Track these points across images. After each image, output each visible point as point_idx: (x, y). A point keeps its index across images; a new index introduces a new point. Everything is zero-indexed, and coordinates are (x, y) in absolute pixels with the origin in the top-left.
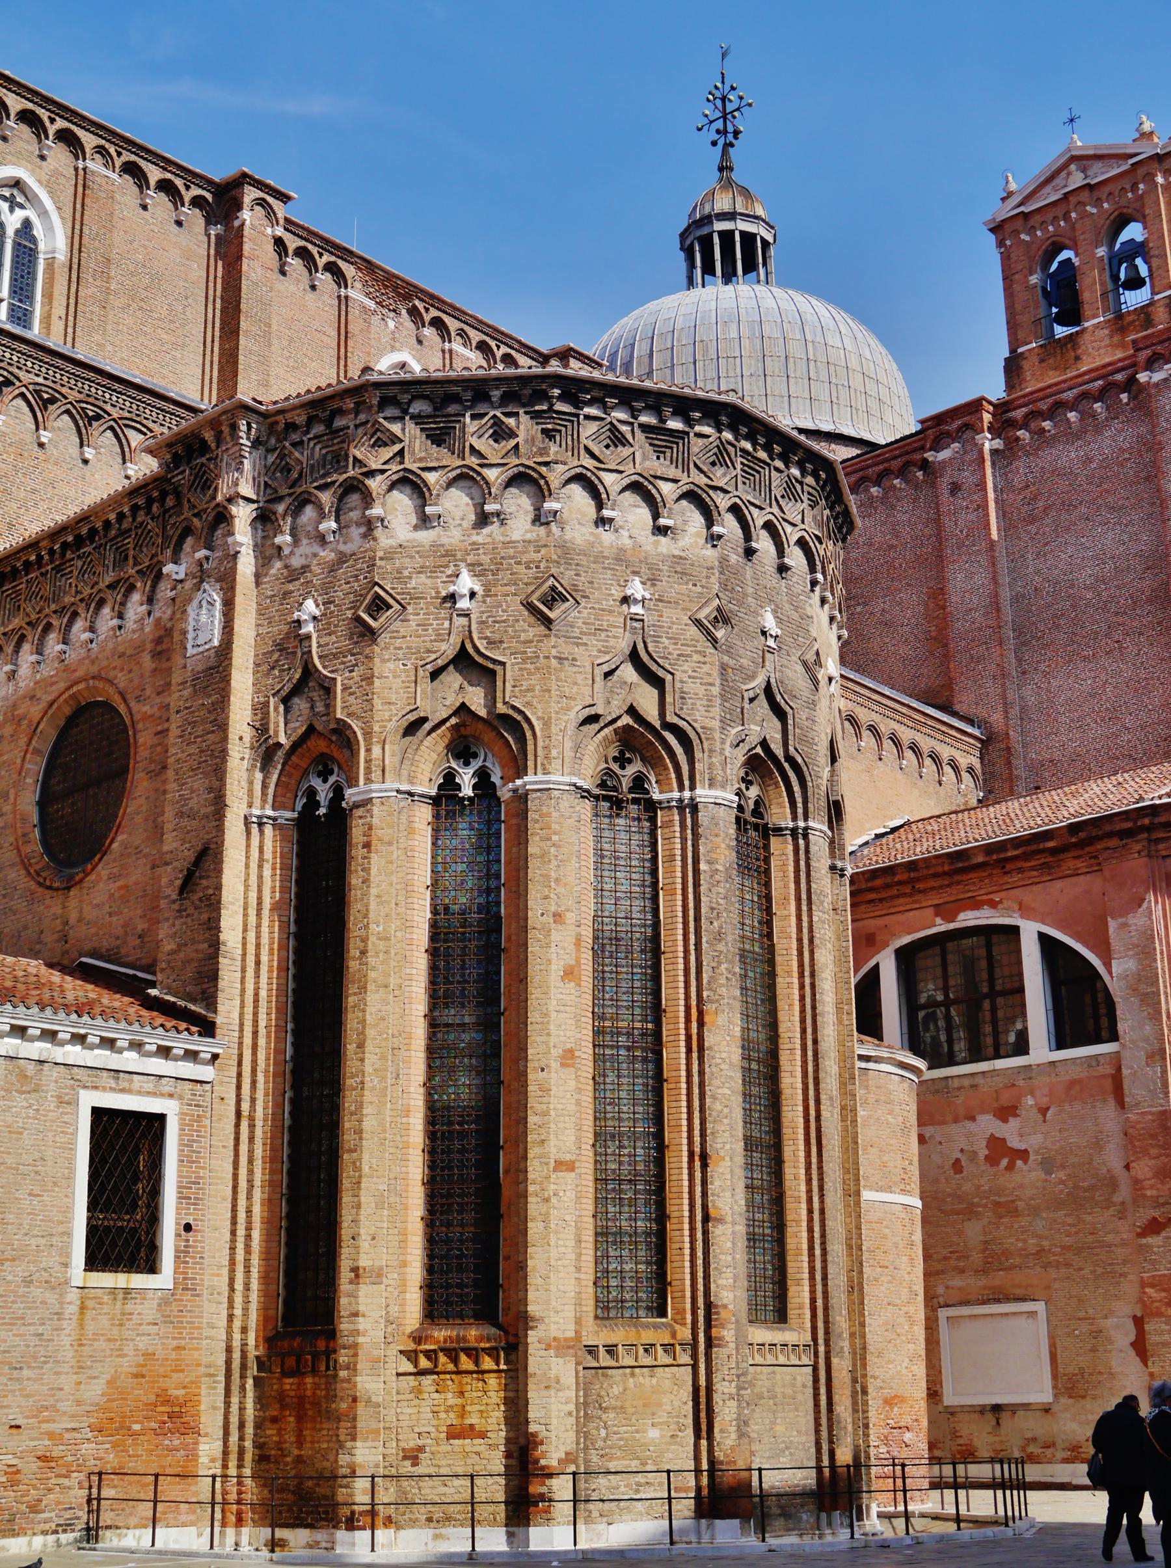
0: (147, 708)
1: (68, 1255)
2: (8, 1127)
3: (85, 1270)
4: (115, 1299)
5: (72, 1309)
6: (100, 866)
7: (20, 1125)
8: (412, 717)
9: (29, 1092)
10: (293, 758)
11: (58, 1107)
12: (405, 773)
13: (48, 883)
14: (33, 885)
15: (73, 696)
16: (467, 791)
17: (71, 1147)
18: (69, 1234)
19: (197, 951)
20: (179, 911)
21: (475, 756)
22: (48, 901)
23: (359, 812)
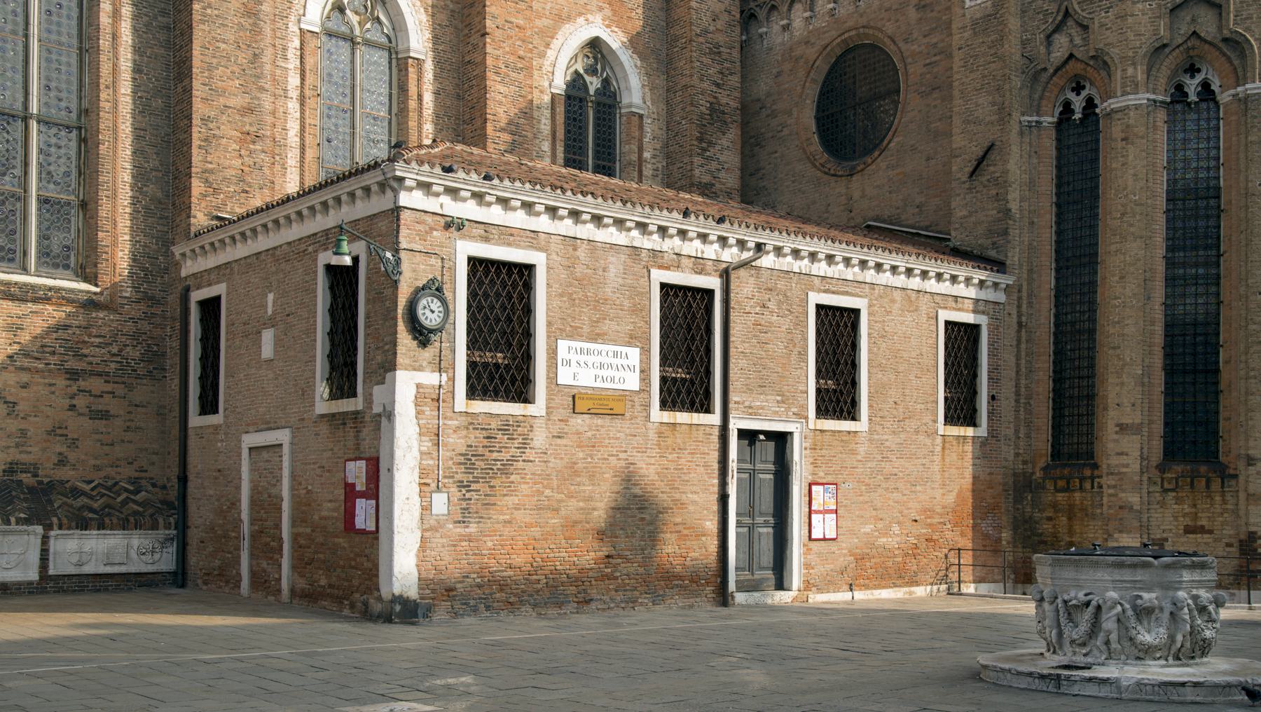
0: (916, 46)
5: (939, 449)
6: (879, 160)
8: (1157, 45)
10: (1054, 78)
12: (1151, 86)
13: (832, 172)
14: (819, 174)
15: (844, 41)
16: (1193, 97)
21: (1199, 71)
23: (1119, 115)
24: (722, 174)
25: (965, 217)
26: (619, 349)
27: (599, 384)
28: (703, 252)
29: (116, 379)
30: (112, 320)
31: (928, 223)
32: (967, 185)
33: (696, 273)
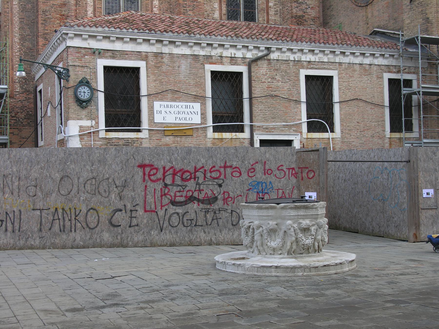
1: (384, 128)
2: (362, 87)
3: (390, 132)
4: (401, 141)
7: (366, 86)
9: (367, 75)
11: (377, 79)
13: (359, 5)
14: (354, 6)
17: (382, 92)
18: (384, 121)
19: (418, 22)
20: (410, 9)
22: (360, 11)
24: (309, 10)
25: (409, 23)
26: (188, 104)
27: (178, 121)
28: (235, 54)
29: (14, 127)
30: (12, 102)
31: (399, 27)
32: (409, 7)
33: (232, 65)
